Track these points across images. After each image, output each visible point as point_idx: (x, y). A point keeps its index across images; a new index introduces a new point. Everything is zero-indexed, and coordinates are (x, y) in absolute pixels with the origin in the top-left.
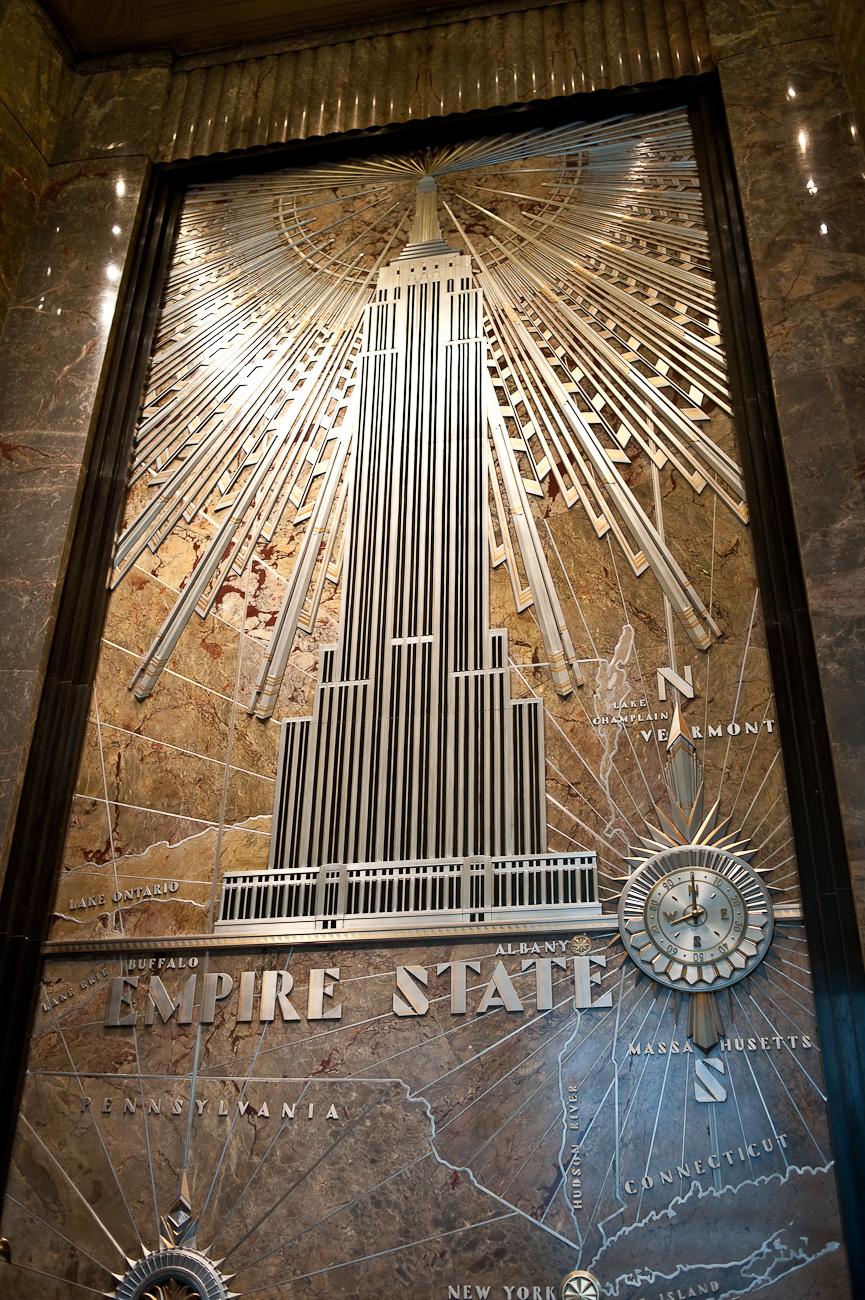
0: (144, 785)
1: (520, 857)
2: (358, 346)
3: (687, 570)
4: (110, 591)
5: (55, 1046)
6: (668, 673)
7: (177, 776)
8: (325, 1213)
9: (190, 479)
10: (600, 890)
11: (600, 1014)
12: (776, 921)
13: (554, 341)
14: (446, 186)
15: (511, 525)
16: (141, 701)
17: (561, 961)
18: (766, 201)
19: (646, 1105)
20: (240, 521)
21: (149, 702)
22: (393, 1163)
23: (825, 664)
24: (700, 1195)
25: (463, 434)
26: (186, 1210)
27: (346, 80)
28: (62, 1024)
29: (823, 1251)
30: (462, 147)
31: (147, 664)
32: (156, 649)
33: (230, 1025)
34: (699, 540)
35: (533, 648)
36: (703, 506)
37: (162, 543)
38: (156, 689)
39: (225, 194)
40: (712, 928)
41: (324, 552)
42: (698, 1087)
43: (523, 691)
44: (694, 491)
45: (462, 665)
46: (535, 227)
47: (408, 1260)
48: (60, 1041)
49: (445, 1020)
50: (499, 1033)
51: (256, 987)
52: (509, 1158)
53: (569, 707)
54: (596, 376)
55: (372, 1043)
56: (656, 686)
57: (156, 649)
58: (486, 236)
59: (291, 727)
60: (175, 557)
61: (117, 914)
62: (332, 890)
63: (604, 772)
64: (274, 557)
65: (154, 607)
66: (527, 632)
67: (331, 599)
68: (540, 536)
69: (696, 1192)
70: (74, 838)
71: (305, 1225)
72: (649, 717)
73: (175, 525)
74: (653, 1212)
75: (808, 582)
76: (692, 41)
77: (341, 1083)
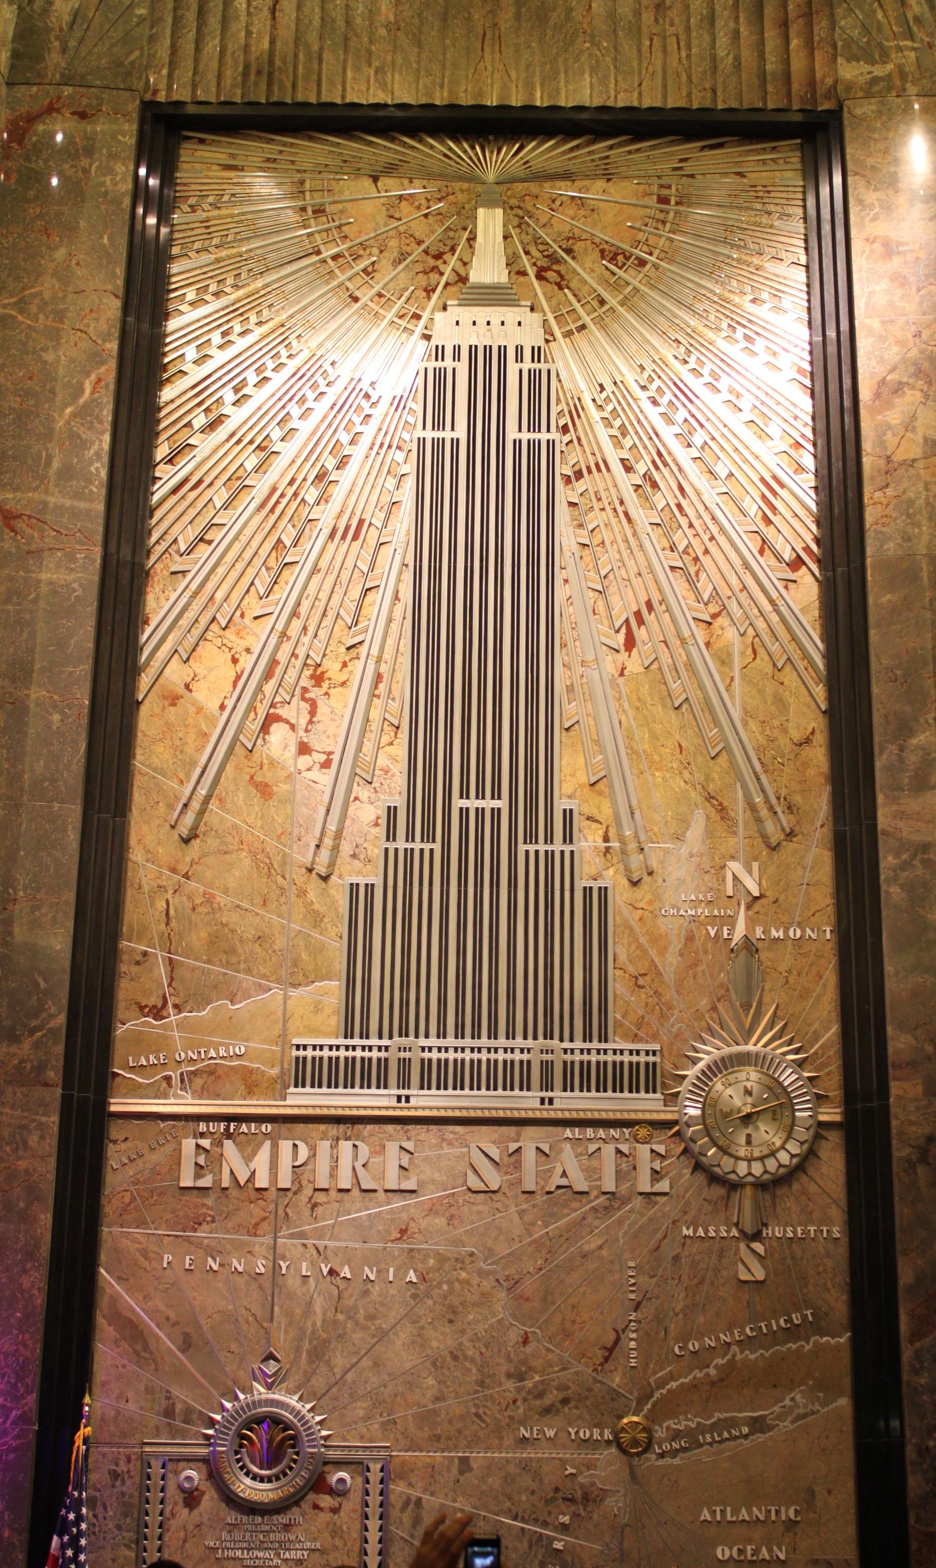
0: (198, 937)
1: (587, 1045)
2: (411, 420)
3: (762, 756)
4: (139, 703)
5: (129, 1205)
6: (735, 866)
7: (233, 931)
8: (408, 1365)
9: (221, 570)
10: (663, 1084)
11: (658, 1198)
12: (821, 1124)
13: (635, 451)
14: (514, 202)
15: (584, 680)
16: (186, 841)
17: (624, 1148)
18: (883, 323)
19: (696, 1281)
20: (284, 634)
21: (196, 843)
22: (469, 1323)
23: (889, 886)
24: (739, 1357)
25: (533, 562)
26: (276, 1360)
27: (392, 18)
28: (134, 1183)
29: (835, 1404)
30: (533, 144)
31: (190, 799)
32: (198, 782)
33: (308, 1191)
34: (776, 723)
35: (604, 826)
36: (782, 683)
37: (194, 650)
38: (202, 828)
39: (233, 156)
40: (762, 1127)
41: (381, 686)
42: (740, 1266)
43: (593, 871)
44: (775, 665)
45: (531, 837)
46: (617, 287)
47: (485, 1406)
48: (133, 1199)
49: (516, 1196)
50: (566, 1211)
51: (332, 1157)
52: (574, 1322)
53: (638, 893)
54: (679, 506)
55: (447, 1214)
56: (724, 880)
57: (198, 782)
58: (561, 288)
59: (354, 888)
60: (211, 670)
61: (182, 1074)
62: (405, 1064)
63: (670, 963)
64: (325, 685)
65: (192, 730)
66: (599, 807)
67: (391, 744)
68: (614, 697)
69: (734, 1356)
70: (125, 991)
71: (389, 1374)
72: (716, 913)
73: (207, 629)
74: (697, 1371)
75: (880, 798)
76: (816, 52)
77: (419, 1250)
